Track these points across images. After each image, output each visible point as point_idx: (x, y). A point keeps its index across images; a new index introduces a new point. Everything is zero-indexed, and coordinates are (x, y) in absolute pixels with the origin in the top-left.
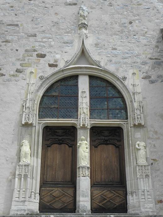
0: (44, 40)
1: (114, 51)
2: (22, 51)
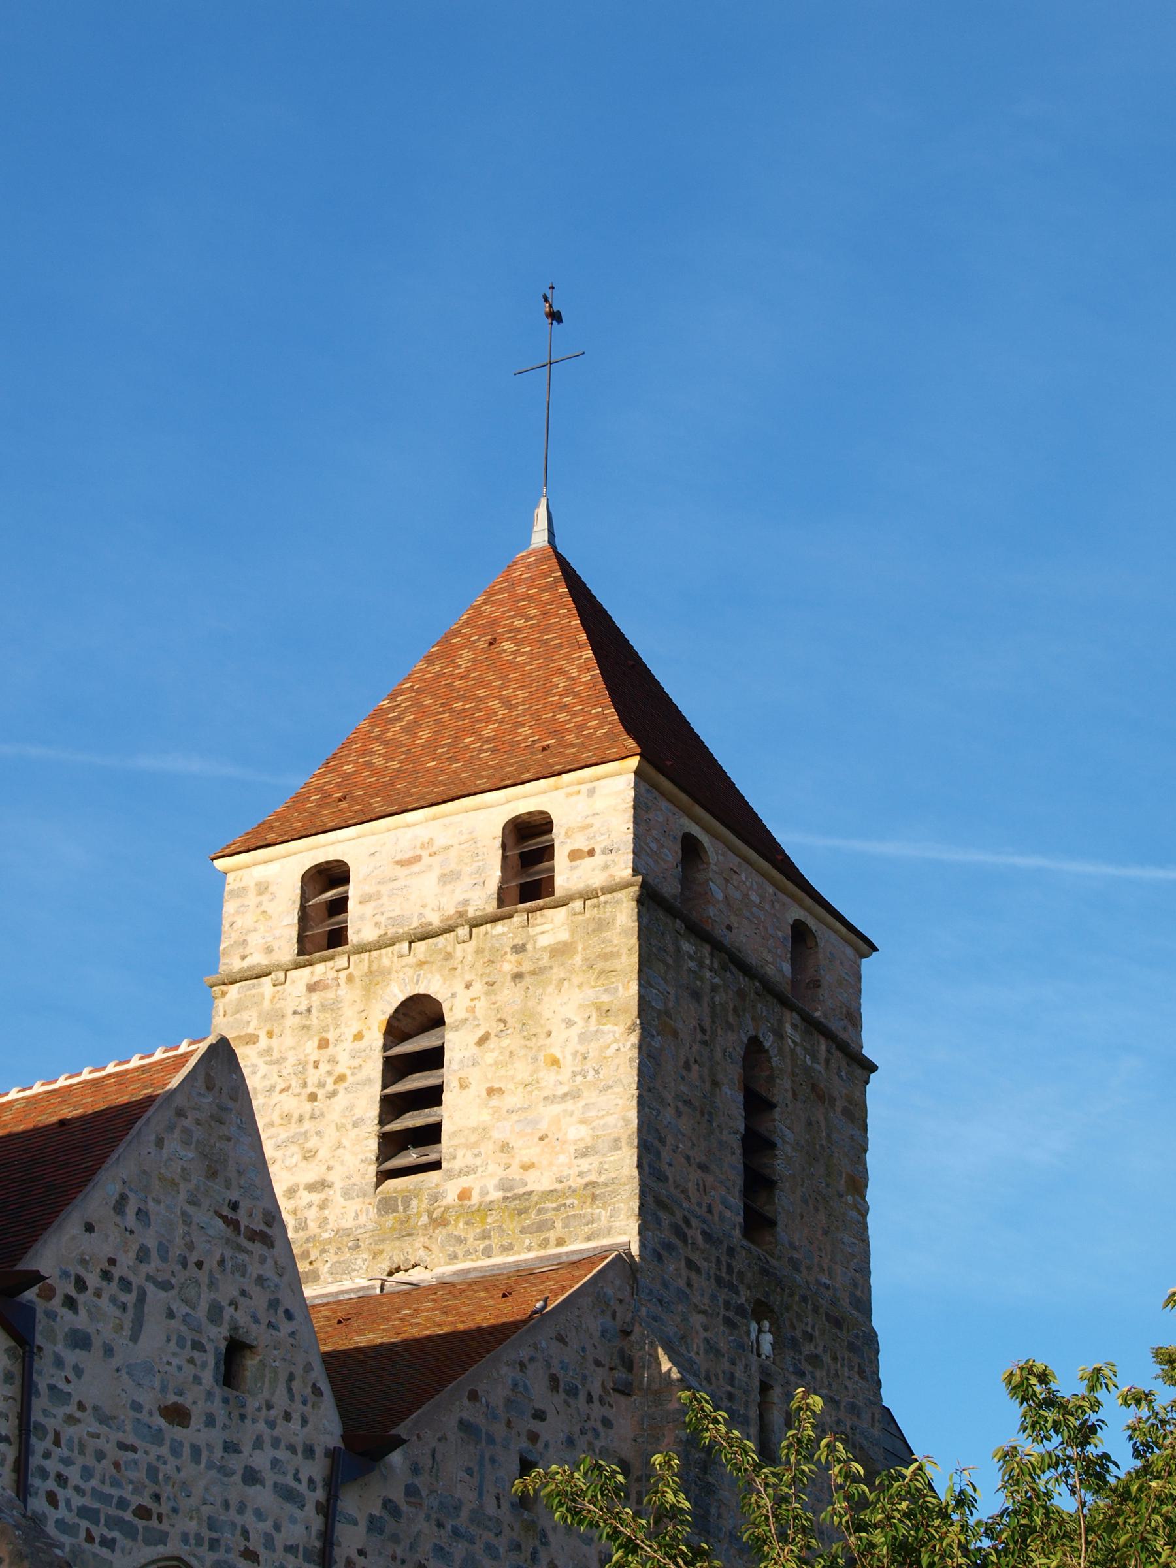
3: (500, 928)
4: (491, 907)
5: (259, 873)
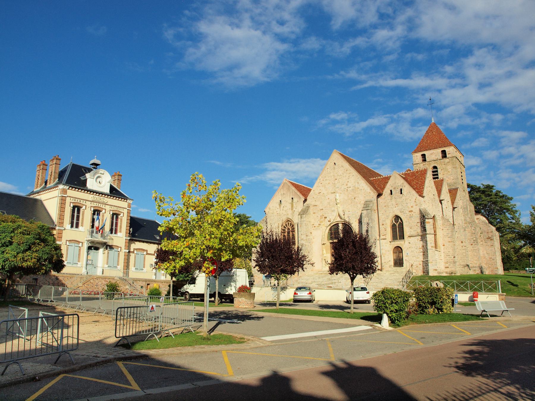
0: (326, 211)
2: (319, 217)
3: (442, 160)
4: (441, 158)
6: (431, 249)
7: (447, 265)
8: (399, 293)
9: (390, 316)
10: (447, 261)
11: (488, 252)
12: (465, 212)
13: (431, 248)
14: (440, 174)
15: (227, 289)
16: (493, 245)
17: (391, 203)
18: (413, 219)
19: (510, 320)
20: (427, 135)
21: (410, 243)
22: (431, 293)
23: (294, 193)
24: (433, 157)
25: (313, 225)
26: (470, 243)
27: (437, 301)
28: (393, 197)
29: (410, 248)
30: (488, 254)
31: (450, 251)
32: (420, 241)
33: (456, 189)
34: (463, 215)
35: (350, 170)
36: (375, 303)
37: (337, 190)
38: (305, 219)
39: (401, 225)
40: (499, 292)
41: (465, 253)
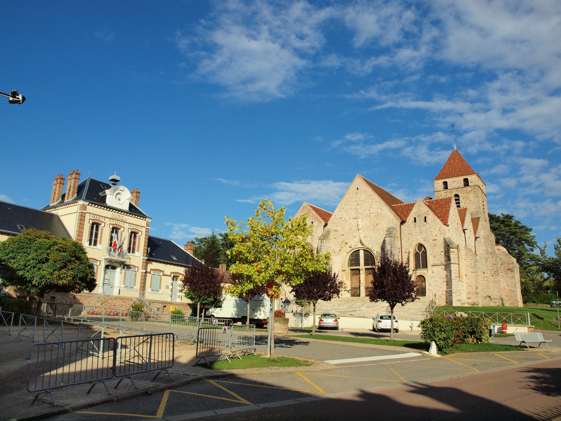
0: (347, 236)
1: (371, 239)
2: (340, 242)
3: (464, 188)
4: (463, 186)
5: (437, 182)
6: (455, 279)
7: (469, 296)
8: (447, 322)
9: (438, 343)
10: (469, 291)
11: (508, 284)
12: (487, 242)
13: (455, 278)
14: (462, 202)
15: (255, 314)
16: (513, 277)
17: (415, 231)
18: (436, 248)
19: (549, 352)
20: (449, 162)
21: (433, 272)
22: (471, 323)
23: (314, 217)
24: (455, 185)
25: (334, 250)
26: (491, 274)
27: (477, 330)
28: (417, 225)
29: (433, 277)
30: (508, 285)
31: (472, 281)
32: (444, 270)
33: (478, 219)
34: (484, 245)
35: (373, 196)
36: (423, 330)
37: (359, 215)
38: (325, 244)
39: (425, 254)
40: (528, 324)
41: (487, 284)
